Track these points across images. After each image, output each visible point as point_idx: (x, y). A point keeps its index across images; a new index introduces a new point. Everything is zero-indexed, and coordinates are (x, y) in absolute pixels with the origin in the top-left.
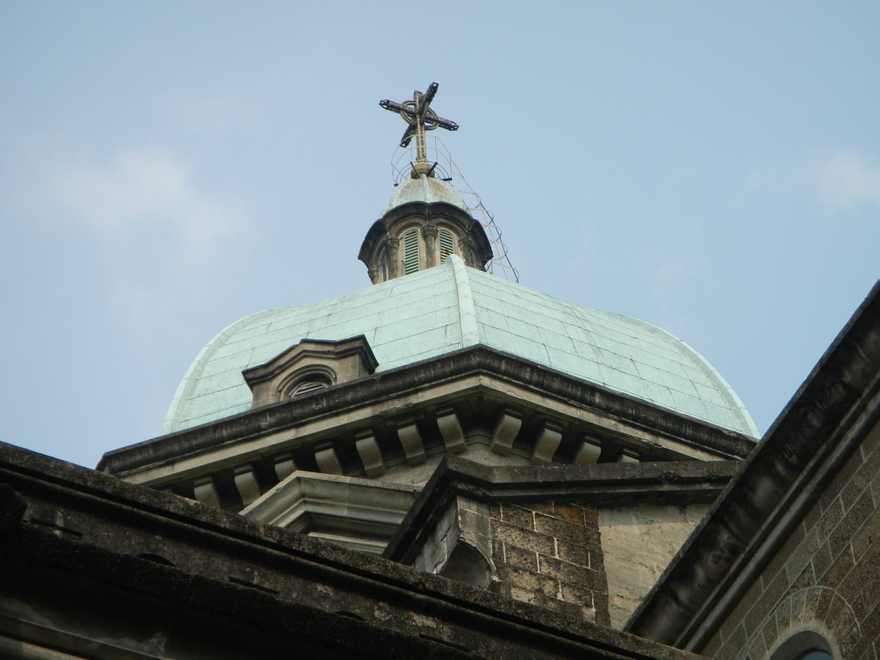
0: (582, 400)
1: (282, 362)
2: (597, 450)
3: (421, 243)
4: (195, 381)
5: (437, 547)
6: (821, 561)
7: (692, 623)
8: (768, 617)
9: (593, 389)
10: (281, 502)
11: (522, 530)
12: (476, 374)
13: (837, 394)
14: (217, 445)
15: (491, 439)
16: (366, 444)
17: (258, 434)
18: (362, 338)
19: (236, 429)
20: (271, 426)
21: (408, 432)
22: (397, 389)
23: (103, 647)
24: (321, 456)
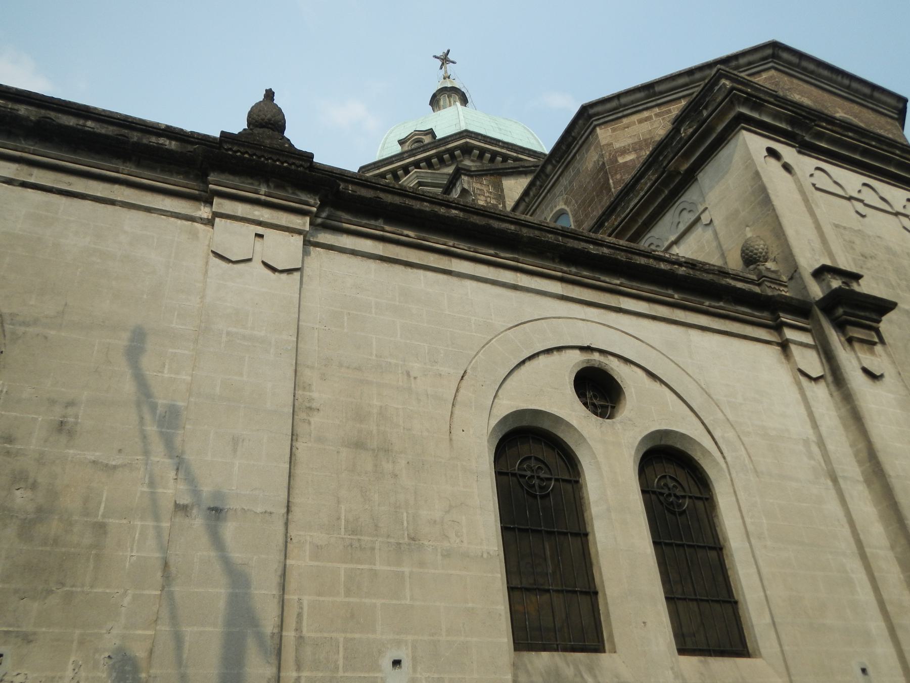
0: (496, 144)
1: (409, 137)
2: (501, 159)
3: (447, 99)
4: (384, 144)
5: (456, 190)
6: (566, 188)
8: (551, 205)
9: (499, 141)
10: (411, 179)
11: (480, 183)
12: (465, 138)
13: (570, 139)
14: (392, 163)
15: (470, 157)
17: (403, 159)
18: (432, 129)
21: (446, 156)
23: (366, 223)
24: (422, 165)
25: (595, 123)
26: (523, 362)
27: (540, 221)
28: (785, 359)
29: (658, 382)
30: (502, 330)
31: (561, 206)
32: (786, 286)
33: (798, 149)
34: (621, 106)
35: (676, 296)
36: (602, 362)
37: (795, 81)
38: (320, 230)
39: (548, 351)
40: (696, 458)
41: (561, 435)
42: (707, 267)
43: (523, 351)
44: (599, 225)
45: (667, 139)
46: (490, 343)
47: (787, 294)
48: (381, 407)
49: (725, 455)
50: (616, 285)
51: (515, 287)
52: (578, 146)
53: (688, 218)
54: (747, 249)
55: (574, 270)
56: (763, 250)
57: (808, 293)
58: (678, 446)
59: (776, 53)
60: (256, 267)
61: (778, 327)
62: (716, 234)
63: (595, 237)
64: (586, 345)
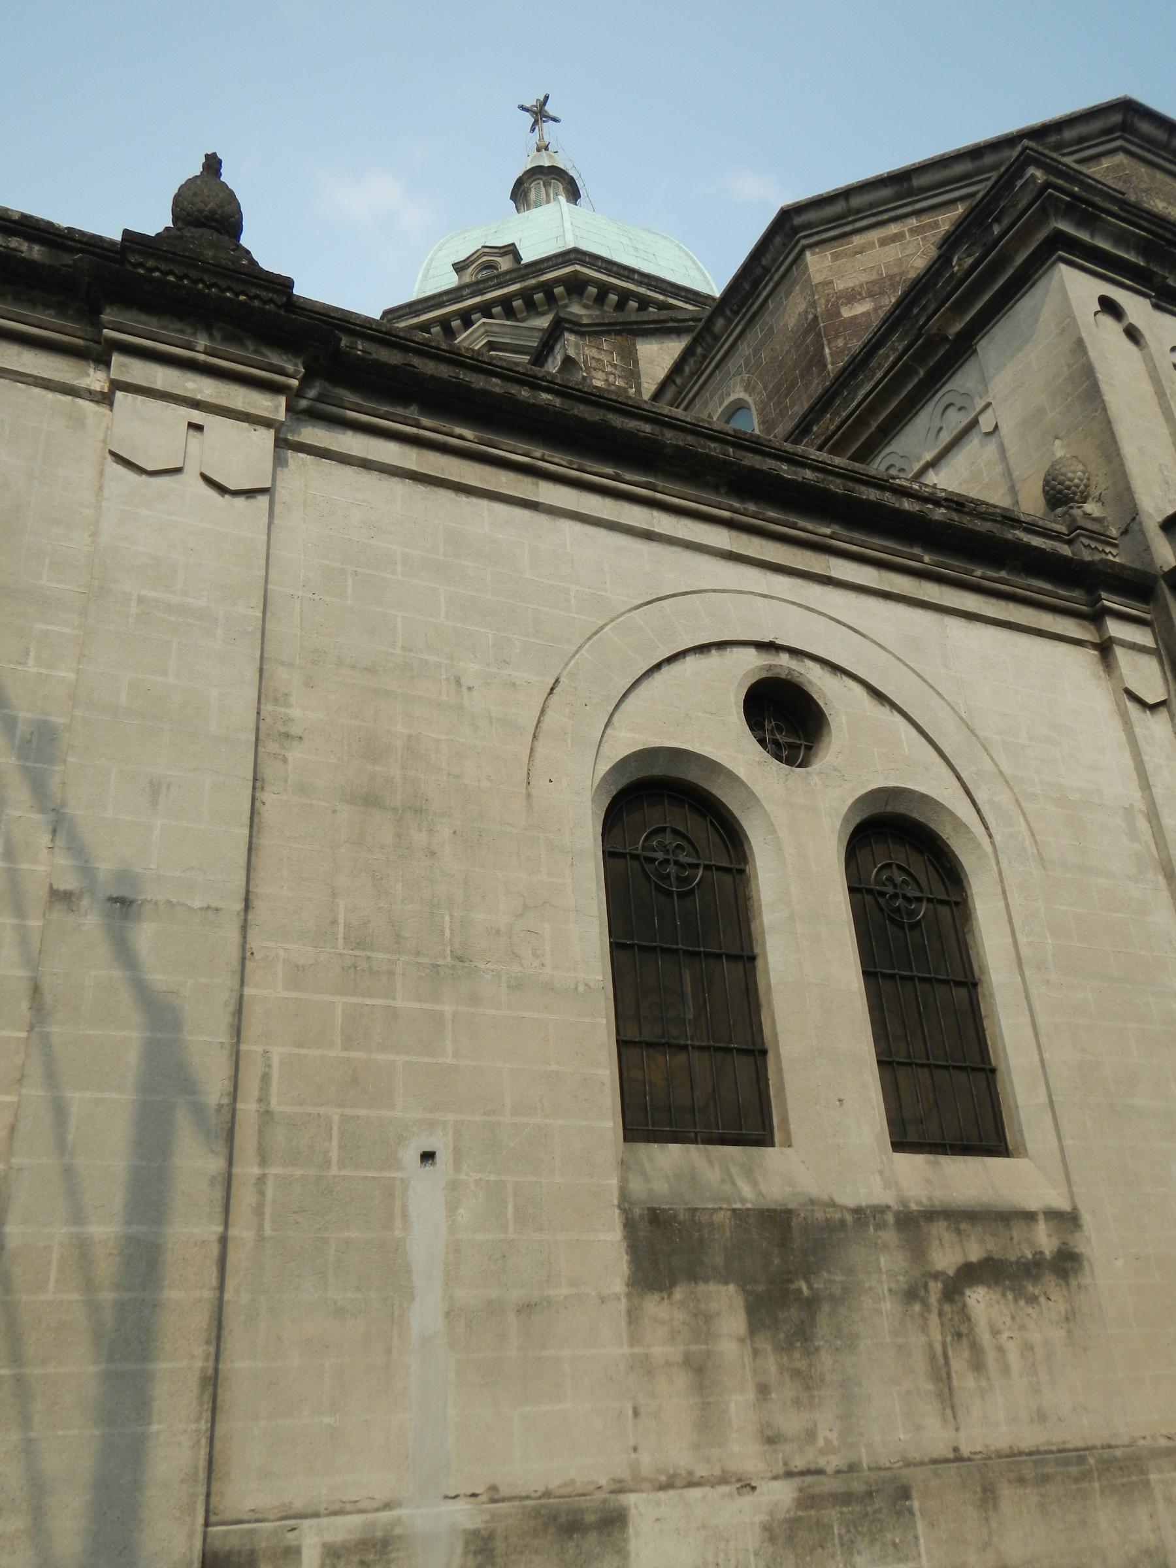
0: (628, 277)
1: (472, 259)
2: (636, 305)
3: (543, 190)
4: (427, 270)
5: (555, 358)
7: (683, 395)
8: (720, 392)
9: (633, 271)
11: (598, 349)
13: (758, 271)
14: (441, 305)
15: (582, 300)
16: (517, 303)
18: (513, 245)
19: (451, 296)
20: (468, 294)
21: (539, 296)
22: (533, 273)
25: (804, 242)
26: (658, 667)
27: (697, 418)
28: (1104, 671)
29: (888, 707)
30: (623, 610)
31: (739, 393)
32: (1115, 546)
33: (1154, 300)
34: (850, 212)
35: (927, 559)
36: (794, 670)
37: (1159, 175)
38: (305, 421)
39: (703, 649)
40: (944, 837)
41: (717, 793)
42: (983, 508)
43: (658, 647)
44: (802, 430)
45: (928, 276)
46: (602, 632)
47: (1117, 560)
48: (410, 736)
49: (993, 831)
50: (825, 536)
51: (649, 536)
52: (771, 285)
53: (956, 421)
54: (1054, 479)
55: (751, 507)
56: (1081, 480)
57: (1152, 559)
58: (915, 815)
59: (1129, 121)
60: (191, 482)
61: (1096, 617)
62: (1002, 450)
63: (791, 450)
64: (766, 640)
